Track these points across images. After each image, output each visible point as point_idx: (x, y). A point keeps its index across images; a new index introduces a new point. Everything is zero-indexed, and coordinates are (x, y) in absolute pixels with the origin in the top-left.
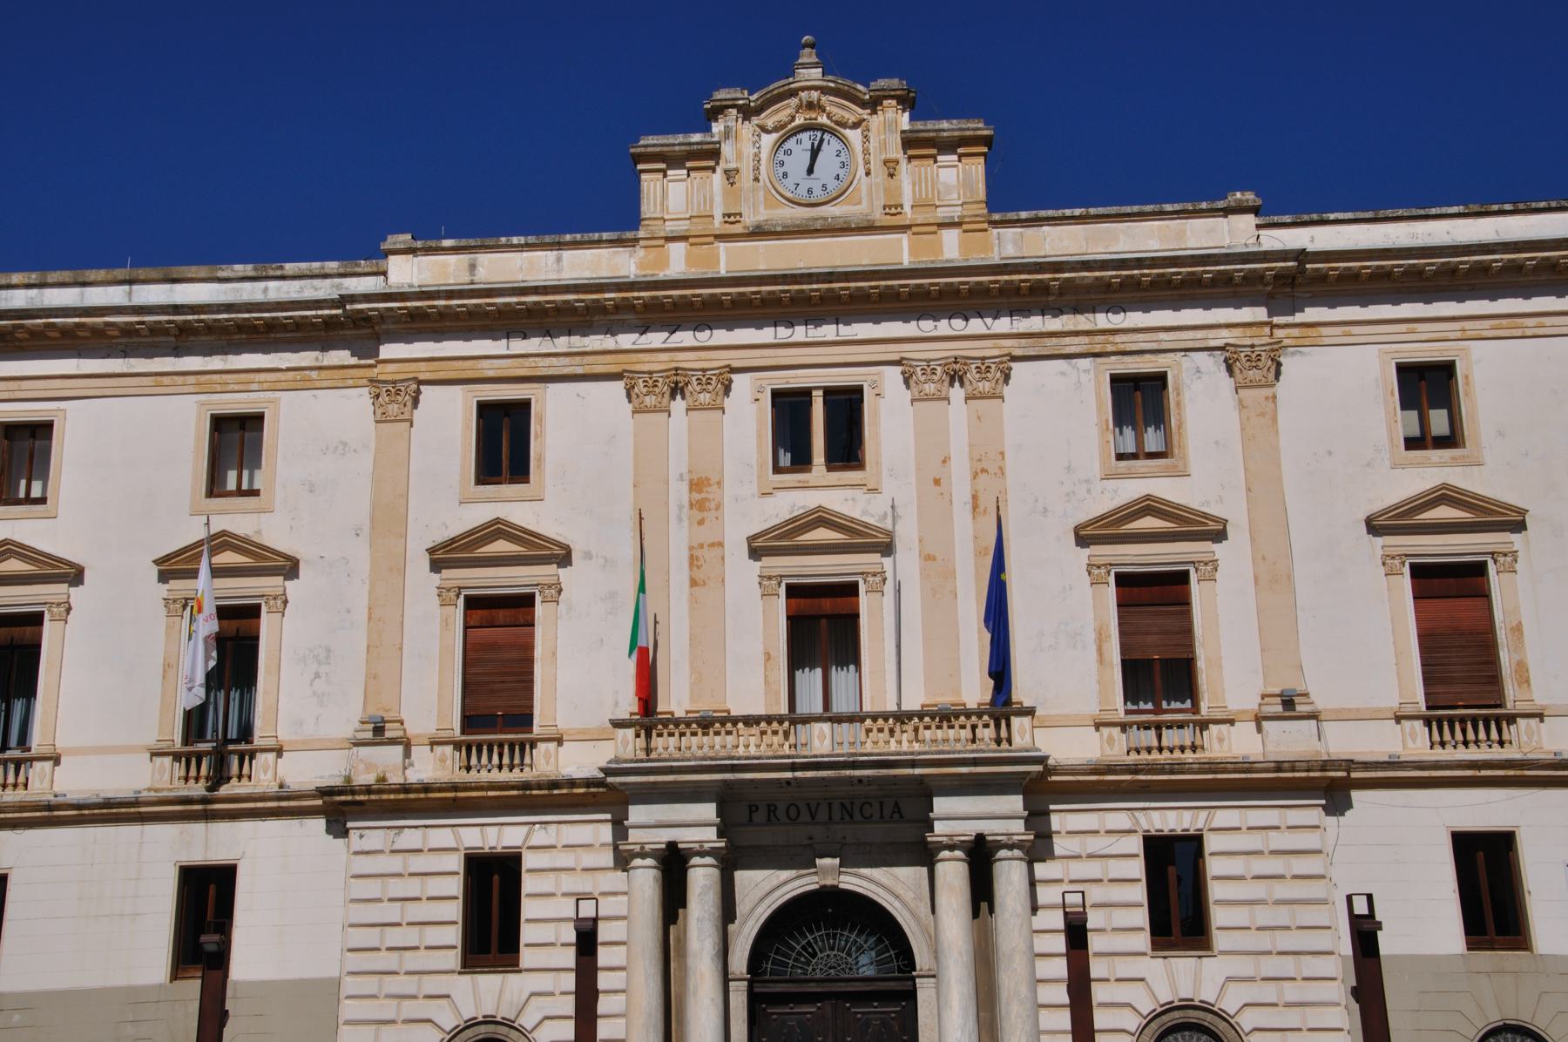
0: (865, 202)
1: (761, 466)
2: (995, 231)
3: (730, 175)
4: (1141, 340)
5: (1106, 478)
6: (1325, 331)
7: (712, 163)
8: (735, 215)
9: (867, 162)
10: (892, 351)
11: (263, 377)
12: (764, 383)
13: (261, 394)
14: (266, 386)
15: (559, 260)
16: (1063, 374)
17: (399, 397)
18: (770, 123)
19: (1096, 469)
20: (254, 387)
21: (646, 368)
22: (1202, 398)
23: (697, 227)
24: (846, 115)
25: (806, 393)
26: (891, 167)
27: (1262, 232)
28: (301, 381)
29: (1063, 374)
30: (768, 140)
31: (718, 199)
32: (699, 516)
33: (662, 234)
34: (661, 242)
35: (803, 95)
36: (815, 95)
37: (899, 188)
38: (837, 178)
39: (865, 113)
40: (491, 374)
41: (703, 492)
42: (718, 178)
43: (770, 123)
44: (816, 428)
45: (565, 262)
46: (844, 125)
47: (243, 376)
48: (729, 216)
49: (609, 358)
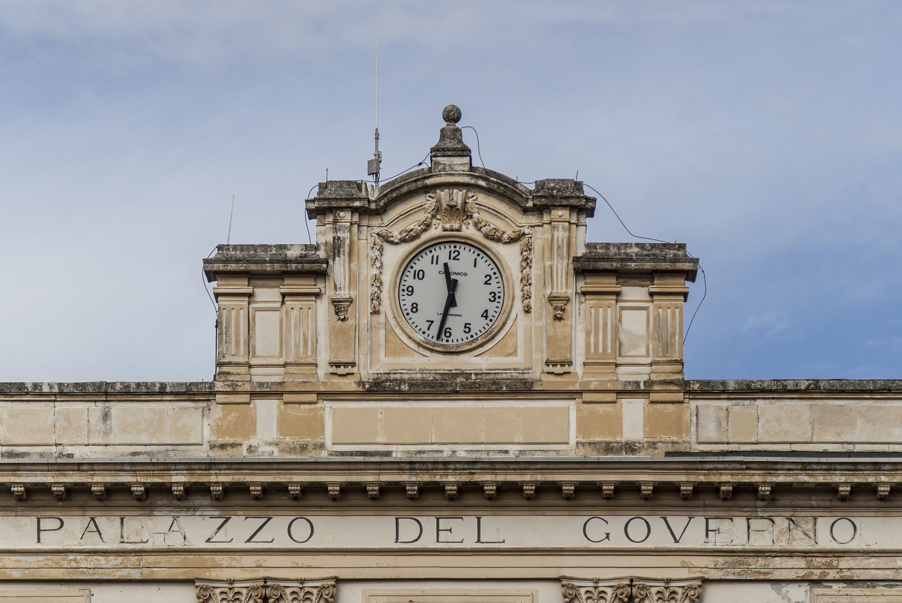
0: (520, 349)
2: (693, 404)
3: (339, 307)
9: (527, 297)
18: (396, 233)
23: (295, 378)
26: (558, 307)
30: (394, 255)
31: (323, 340)
33: (247, 387)
34: (246, 398)
38: (485, 315)
42: (323, 307)
43: (396, 233)
45: (114, 421)
48: (338, 365)
49: (176, 559)
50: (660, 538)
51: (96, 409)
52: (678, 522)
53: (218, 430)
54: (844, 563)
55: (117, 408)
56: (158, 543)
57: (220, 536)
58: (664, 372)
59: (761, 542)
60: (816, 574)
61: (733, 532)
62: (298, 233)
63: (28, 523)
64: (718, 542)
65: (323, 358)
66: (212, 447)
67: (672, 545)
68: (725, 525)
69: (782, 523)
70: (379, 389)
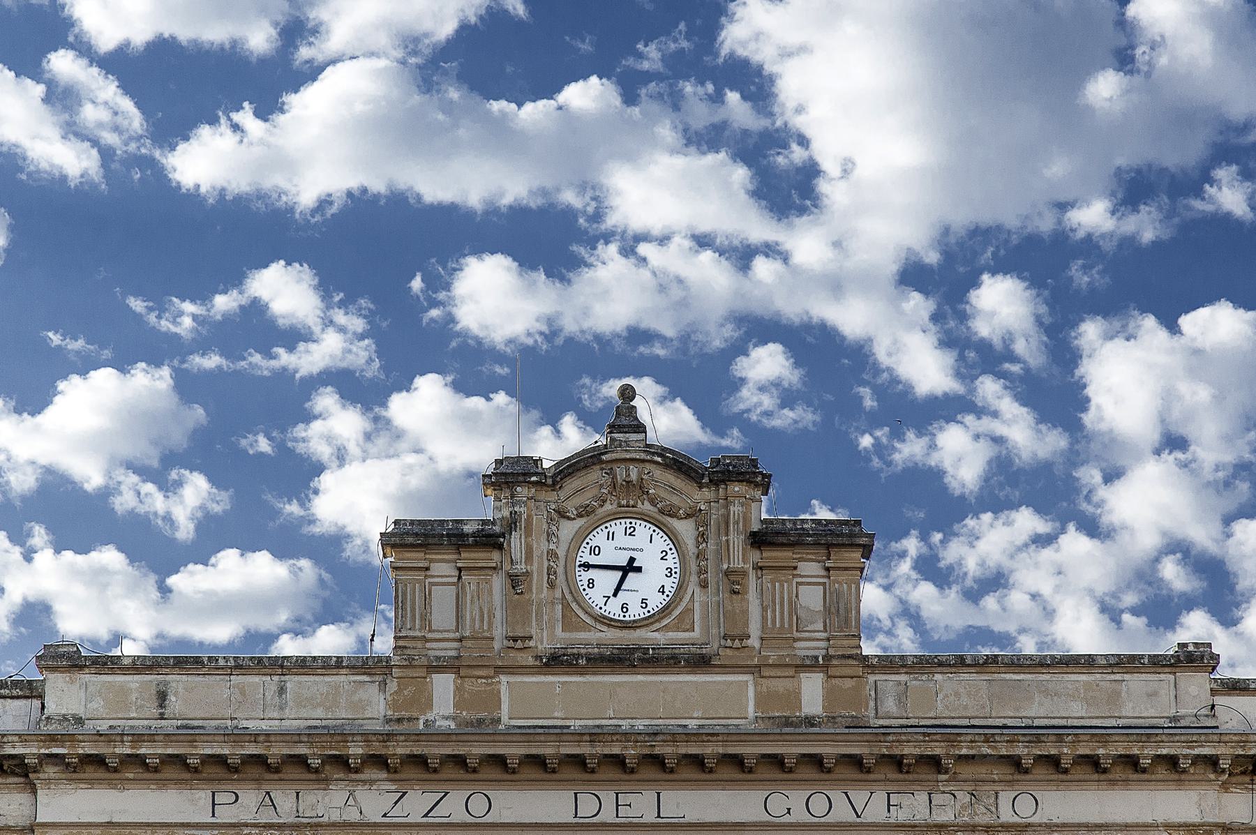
2: (872, 678)
3: (515, 581)
8: (524, 638)
15: (282, 690)
24: (675, 500)
27: (1219, 700)
33: (424, 661)
37: (745, 612)
38: (662, 590)
39: (701, 497)
42: (498, 583)
48: (515, 640)
51: (272, 682)
52: (859, 797)
53: (394, 705)
55: (292, 682)
57: (397, 811)
63: (203, 796)
64: (900, 816)
65: (499, 631)
66: (388, 721)
67: (852, 817)
68: (906, 800)
70: (556, 662)
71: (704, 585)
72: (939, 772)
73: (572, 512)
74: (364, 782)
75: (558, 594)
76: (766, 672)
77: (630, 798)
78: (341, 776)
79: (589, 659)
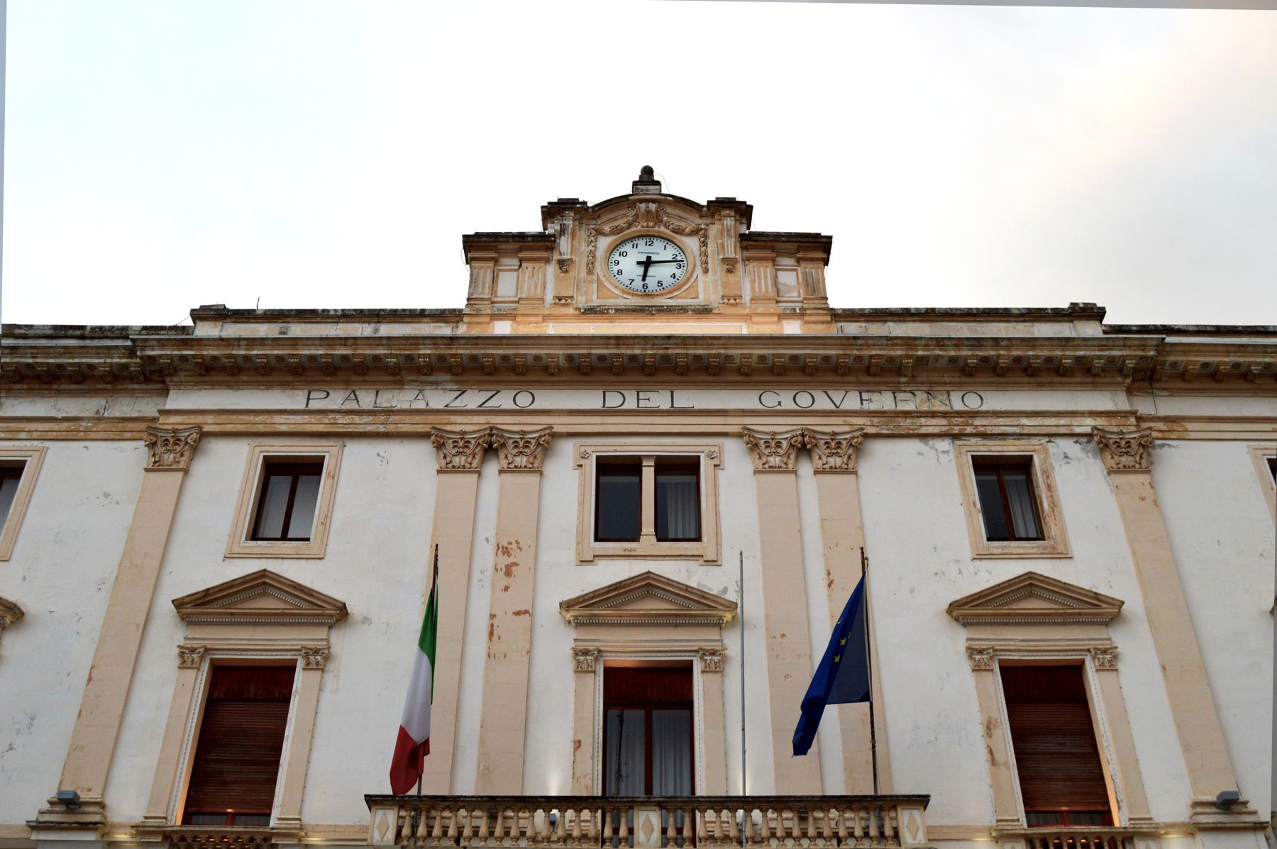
1: (581, 534)
3: (561, 263)
4: (1003, 425)
5: (979, 557)
6: (1190, 426)
7: (545, 255)
10: (734, 424)
11: (33, 426)
12: (589, 450)
13: (28, 443)
14: (35, 435)
16: (920, 454)
17: (174, 448)
19: (967, 552)
20: (23, 435)
21: (457, 428)
22: (1076, 486)
24: (683, 225)
25: (632, 466)
28: (73, 430)
29: (920, 454)
32: (505, 581)
34: (487, 319)
35: (643, 206)
36: (653, 207)
39: (701, 223)
40: (284, 428)
41: (511, 560)
42: (551, 270)
44: (644, 497)
46: (679, 231)
47: (13, 425)
49: (418, 418)
50: (822, 403)
54: (977, 422)
56: (406, 406)
58: (817, 304)
59: (910, 407)
60: (956, 430)
61: (883, 401)
62: (533, 224)
67: (833, 408)
68: (875, 397)
69: (921, 396)
71: (706, 271)
72: (900, 375)
73: (607, 229)
74: (432, 383)
75: (595, 277)
76: (755, 319)
77: (649, 395)
78: (414, 378)
79: (617, 310)
